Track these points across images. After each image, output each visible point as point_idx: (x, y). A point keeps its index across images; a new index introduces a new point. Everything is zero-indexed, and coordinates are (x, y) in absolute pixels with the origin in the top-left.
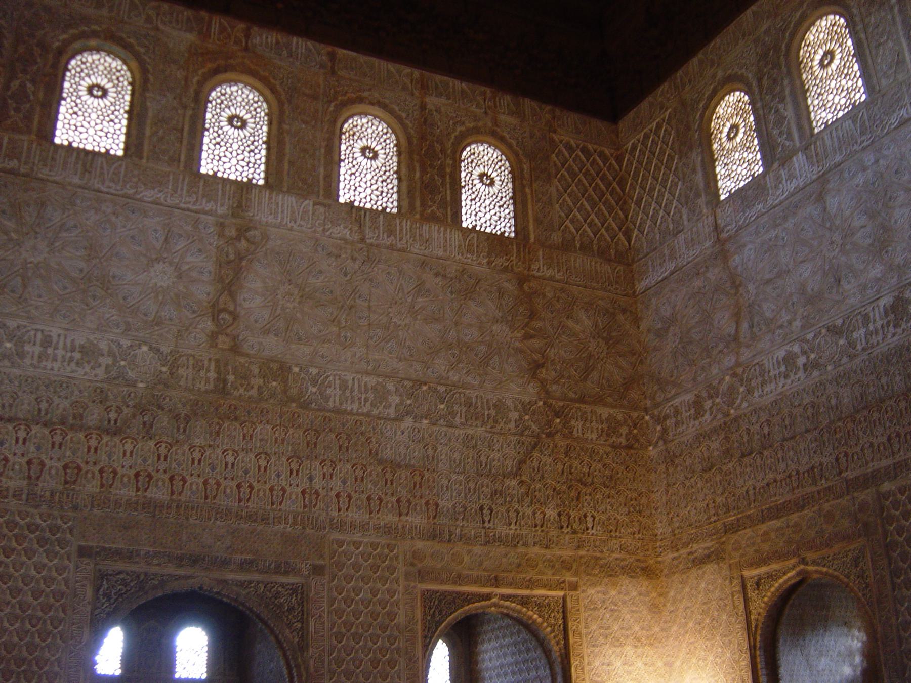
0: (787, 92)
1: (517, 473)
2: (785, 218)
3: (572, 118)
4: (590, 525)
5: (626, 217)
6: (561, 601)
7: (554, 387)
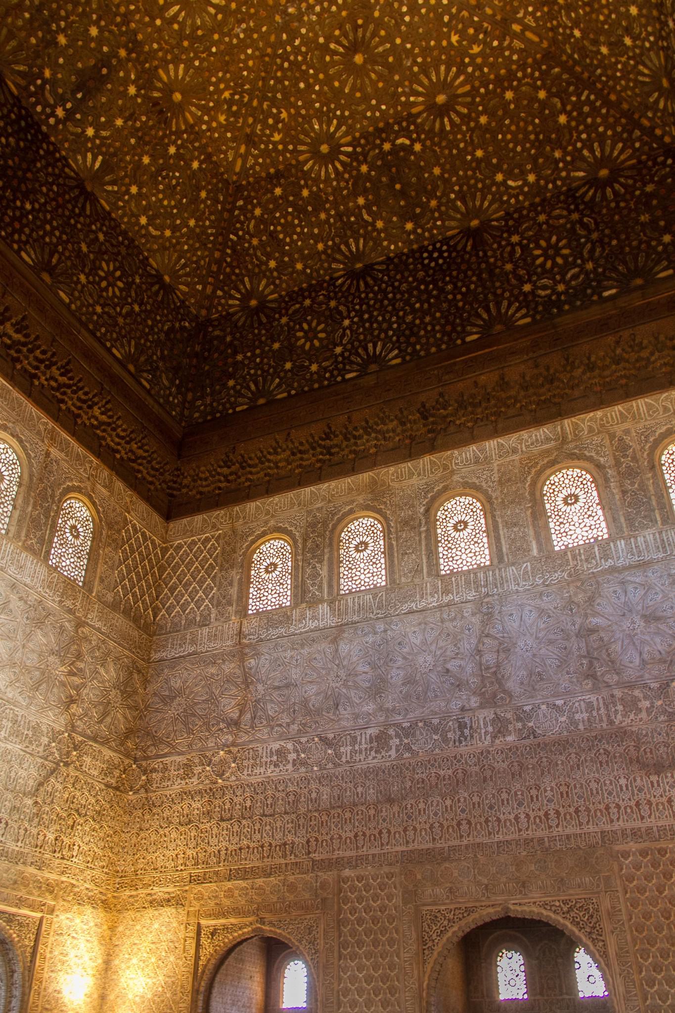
0: (326, 557)
1: (35, 793)
2: (302, 646)
3: (143, 506)
4: (75, 854)
5: (158, 597)
6: (38, 922)
7: (79, 722)
